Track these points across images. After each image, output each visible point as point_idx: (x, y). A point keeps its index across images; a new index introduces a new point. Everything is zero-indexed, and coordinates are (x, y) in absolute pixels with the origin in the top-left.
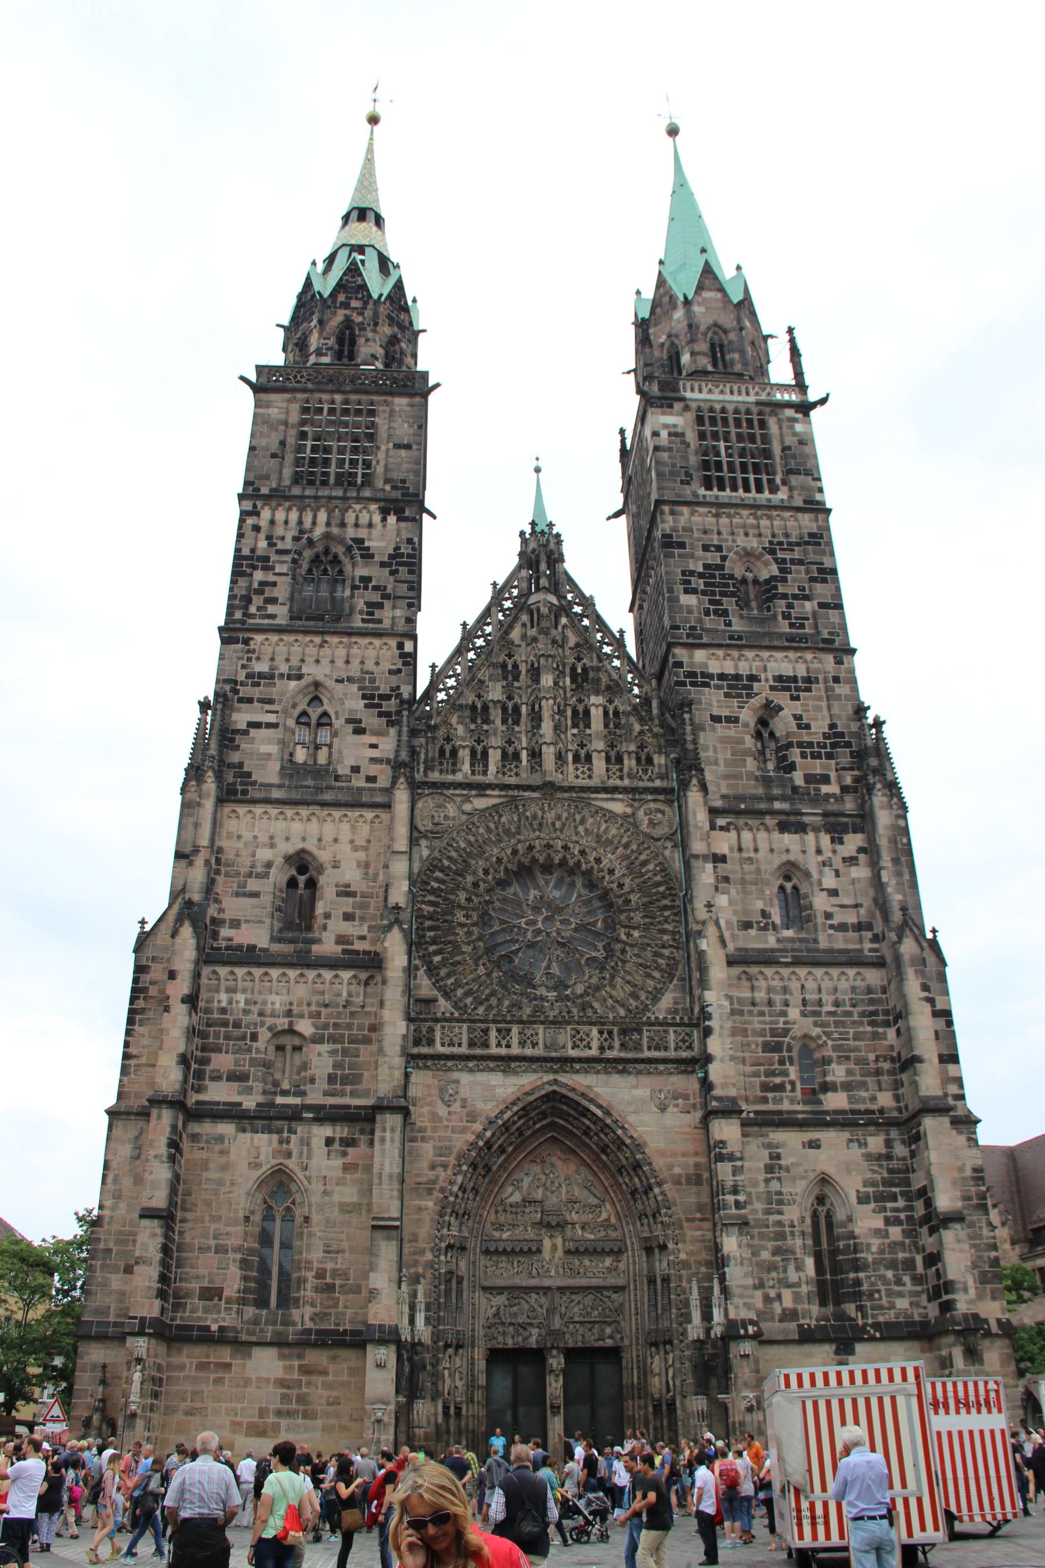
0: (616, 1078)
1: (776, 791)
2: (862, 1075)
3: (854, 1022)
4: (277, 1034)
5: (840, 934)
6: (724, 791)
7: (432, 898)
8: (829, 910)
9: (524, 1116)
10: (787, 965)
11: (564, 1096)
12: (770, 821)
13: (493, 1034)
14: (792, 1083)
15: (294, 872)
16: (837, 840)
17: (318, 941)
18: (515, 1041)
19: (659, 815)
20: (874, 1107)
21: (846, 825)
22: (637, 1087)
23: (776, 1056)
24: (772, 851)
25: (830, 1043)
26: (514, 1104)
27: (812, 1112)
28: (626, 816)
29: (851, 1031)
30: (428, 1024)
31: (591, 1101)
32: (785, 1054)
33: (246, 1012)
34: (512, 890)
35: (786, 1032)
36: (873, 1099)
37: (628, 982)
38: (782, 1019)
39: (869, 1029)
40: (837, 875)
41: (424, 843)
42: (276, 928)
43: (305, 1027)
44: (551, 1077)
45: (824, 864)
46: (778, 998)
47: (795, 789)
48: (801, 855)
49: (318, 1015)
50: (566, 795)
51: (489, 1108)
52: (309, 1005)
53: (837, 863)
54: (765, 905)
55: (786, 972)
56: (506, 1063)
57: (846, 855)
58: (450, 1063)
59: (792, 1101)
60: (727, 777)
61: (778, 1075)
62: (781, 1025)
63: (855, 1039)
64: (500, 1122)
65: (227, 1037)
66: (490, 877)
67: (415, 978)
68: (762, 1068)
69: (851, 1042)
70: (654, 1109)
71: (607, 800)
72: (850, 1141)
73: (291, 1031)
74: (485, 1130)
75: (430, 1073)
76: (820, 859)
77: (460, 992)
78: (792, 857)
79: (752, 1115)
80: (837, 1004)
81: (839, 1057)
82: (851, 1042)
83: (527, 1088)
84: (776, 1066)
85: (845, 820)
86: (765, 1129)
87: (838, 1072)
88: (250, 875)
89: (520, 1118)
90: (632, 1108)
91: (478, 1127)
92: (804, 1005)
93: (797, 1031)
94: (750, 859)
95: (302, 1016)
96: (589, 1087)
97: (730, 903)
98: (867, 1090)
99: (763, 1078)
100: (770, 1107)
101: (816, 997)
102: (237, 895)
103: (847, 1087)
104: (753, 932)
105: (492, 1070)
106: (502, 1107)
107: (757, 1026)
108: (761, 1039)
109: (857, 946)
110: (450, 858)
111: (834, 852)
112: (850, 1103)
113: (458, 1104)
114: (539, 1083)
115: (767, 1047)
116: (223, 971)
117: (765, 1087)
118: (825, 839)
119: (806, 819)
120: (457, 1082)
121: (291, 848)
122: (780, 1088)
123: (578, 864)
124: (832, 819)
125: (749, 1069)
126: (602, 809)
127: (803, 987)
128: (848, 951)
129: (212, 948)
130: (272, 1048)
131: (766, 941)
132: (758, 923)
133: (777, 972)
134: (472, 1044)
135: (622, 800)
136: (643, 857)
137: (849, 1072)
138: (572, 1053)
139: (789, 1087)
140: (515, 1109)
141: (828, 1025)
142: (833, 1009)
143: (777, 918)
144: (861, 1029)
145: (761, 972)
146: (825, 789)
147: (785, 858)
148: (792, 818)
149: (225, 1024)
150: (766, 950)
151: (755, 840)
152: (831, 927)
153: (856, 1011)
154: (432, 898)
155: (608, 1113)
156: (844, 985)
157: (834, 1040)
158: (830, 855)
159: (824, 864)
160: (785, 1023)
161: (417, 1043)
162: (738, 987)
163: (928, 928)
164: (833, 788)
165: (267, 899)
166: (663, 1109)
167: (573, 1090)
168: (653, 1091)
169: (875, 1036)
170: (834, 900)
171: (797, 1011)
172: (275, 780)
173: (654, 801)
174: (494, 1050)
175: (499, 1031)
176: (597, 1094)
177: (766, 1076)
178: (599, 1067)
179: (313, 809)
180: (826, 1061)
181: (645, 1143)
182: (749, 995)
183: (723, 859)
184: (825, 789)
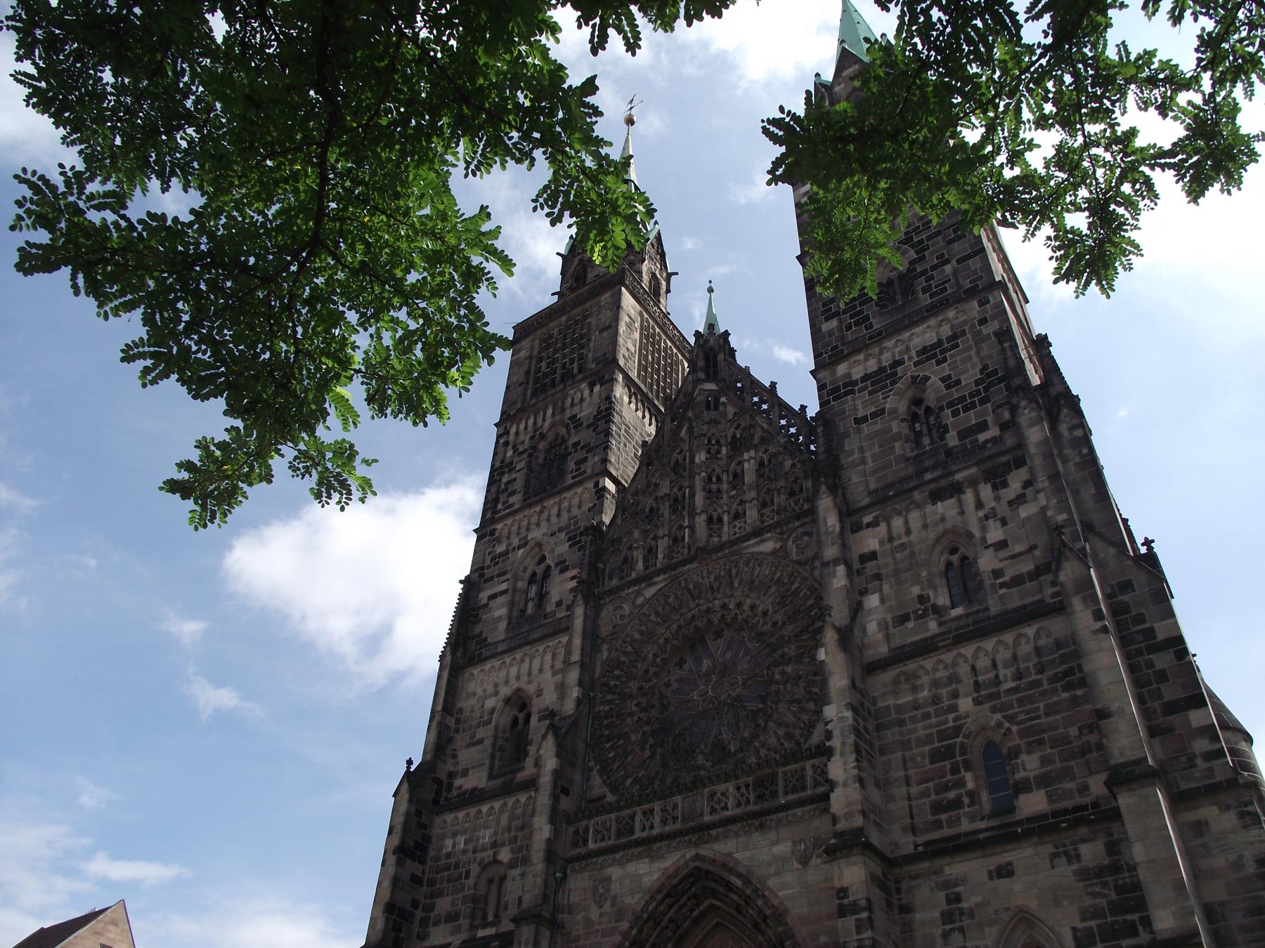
0: (757, 837)
1: (928, 463)
2: (1065, 760)
3: (1044, 693)
4: (484, 867)
5: (1014, 590)
6: (873, 487)
7: (609, 697)
8: (998, 566)
9: (674, 903)
10: (948, 648)
11: (708, 872)
12: (917, 496)
13: (638, 817)
14: (971, 794)
15: (515, 712)
16: (999, 483)
17: (522, 769)
18: (657, 819)
19: (806, 538)
20: (1087, 800)
21: (1008, 463)
22: (777, 842)
23: (947, 764)
24: (925, 526)
25: (1014, 728)
26: (658, 891)
27: (999, 827)
28: (775, 552)
29: (1042, 705)
30: (584, 823)
31: (731, 871)
32: (959, 758)
33: (464, 851)
34: (686, 666)
35: (957, 730)
36: (1084, 789)
37: (780, 725)
38: (951, 716)
39: (1065, 695)
40: (1004, 522)
41: (605, 647)
42: (496, 767)
43: (505, 855)
44: (693, 852)
45: (987, 517)
46: (944, 692)
47: (949, 452)
48: (959, 518)
49: (516, 837)
50: (720, 554)
51: (633, 901)
52: (509, 830)
53: (1003, 509)
54: (922, 589)
55: (948, 657)
56: (649, 846)
57: (1012, 496)
58: (601, 859)
59: (972, 819)
60: (874, 472)
61: (952, 788)
62: (951, 724)
63: (1047, 714)
64: (645, 916)
65: (449, 881)
66: (659, 660)
67: (588, 780)
68: (931, 784)
69: (1043, 720)
70: (796, 865)
71: (758, 544)
72: (1054, 856)
73: (496, 861)
74: (631, 928)
75: (586, 875)
76: (981, 514)
77: (629, 781)
78: (948, 525)
79: (921, 849)
80: (1019, 676)
81: (1029, 744)
82: (1043, 720)
83: (671, 871)
84: (949, 777)
85: (1004, 459)
86: (939, 862)
87: (1030, 765)
88: (478, 726)
89: (670, 907)
90: (772, 870)
91: (625, 925)
92: (977, 691)
93: (971, 725)
94: (903, 546)
95: (503, 845)
96: (730, 855)
97: (882, 601)
98: (1073, 779)
99: (933, 797)
100: (946, 832)
101: (991, 675)
102: (469, 746)
103: (1044, 781)
104: (910, 625)
105: (639, 857)
106: (647, 898)
107: (922, 733)
108: (927, 748)
109: (1038, 597)
110: (626, 654)
111: (997, 499)
112: (1051, 801)
113: (608, 904)
114: (682, 862)
115: (936, 756)
116: (449, 817)
117: (937, 808)
118: (986, 491)
119: (959, 476)
120: (609, 879)
121: (505, 691)
122: (956, 804)
123: (735, 618)
124: (989, 464)
125: (914, 790)
126: (753, 554)
127: (973, 668)
128: (1026, 606)
129: (447, 799)
130: (483, 882)
131: (927, 630)
132: (915, 612)
133: (940, 661)
134: (619, 834)
135: (770, 538)
136: (794, 587)
137: (1045, 761)
138: (707, 818)
139: (966, 800)
140: (660, 897)
141: (1011, 707)
142: (1013, 684)
143: (943, 600)
144: (1055, 699)
145: (922, 667)
146: (982, 437)
147: (940, 528)
148: (944, 483)
149: (448, 867)
150: (925, 640)
151: (906, 522)
152: (1003, 585)
153: (1043, 677)
154: (609, 697)
155: (747, 881)
156: (1025, 649)
157: (1019, 723)
158: (993, 504)
159: (987, 517)
160: (955, 720)
161: (576, 844)
162: (895, 693)
163: (1139, 540)
164: (993, 432)
165: (488, 743)
166: (805, 862)
167: (714, 861)
168: (795, 843)
169: (1074, 701)
170: (1003, 554)
171: (969, 700)
172: (502, 637)
173: (803, 525)
174: (638, 834)
175: (644, 813)
176: (737, 861)
177: (937, 793)
178: (734, 827)
179: (526, 649)
180: (1015, 753)
181: (787, 910)
182: (910, 698)
183: (873, 556)
184: (982, 437)
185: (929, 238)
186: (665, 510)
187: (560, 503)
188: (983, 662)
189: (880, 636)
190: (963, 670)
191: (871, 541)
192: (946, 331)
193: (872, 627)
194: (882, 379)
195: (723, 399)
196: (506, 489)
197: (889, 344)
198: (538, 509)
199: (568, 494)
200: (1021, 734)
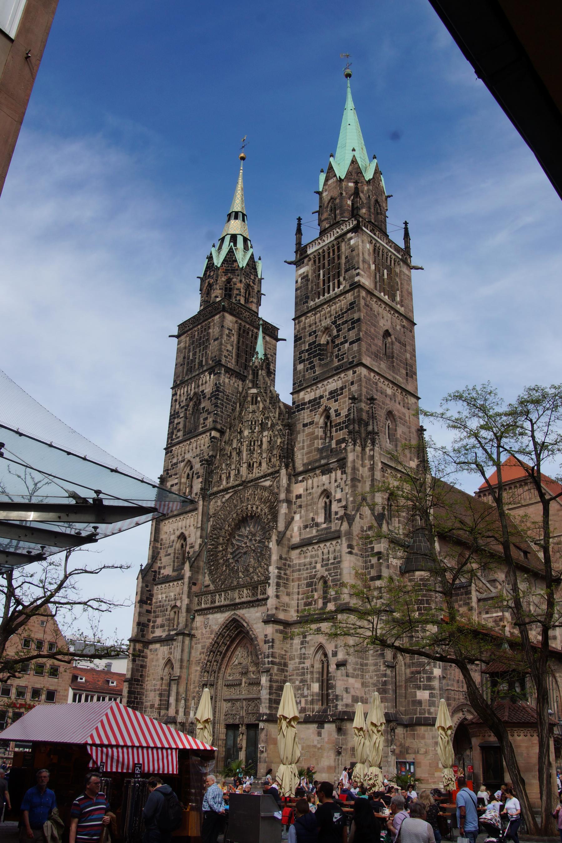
6: (305, 461)
60: (307, 454)
104: (308, 529)
185: (343, 323)
186: (234, 454)
187: (197, 441)
188: (326, 551)
189: (298, 533)
190: (320, 552)
191: (299, 489)
192: (339, 384)
193: (296, 529)
194: (315, 403)
195: (259, 399)
196: (176, 428)
197: (320, 385)
198: (188, 442)
199: (200, 437)
200: (333, 581)
